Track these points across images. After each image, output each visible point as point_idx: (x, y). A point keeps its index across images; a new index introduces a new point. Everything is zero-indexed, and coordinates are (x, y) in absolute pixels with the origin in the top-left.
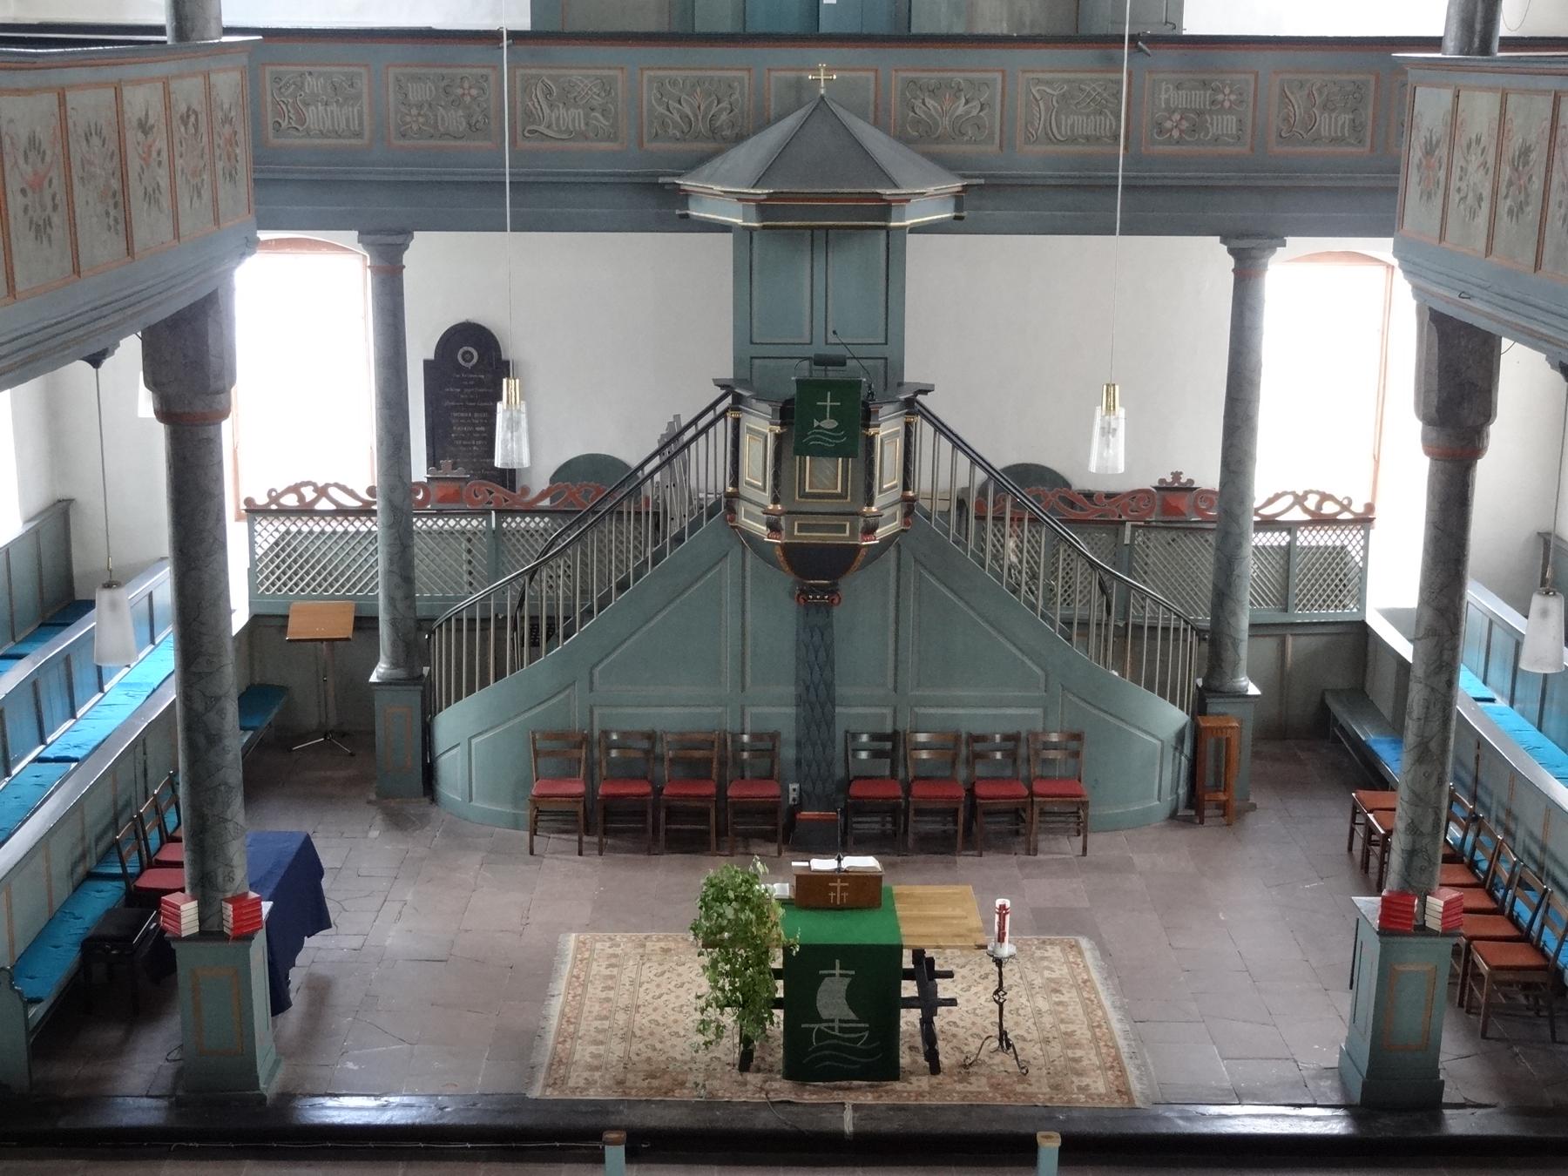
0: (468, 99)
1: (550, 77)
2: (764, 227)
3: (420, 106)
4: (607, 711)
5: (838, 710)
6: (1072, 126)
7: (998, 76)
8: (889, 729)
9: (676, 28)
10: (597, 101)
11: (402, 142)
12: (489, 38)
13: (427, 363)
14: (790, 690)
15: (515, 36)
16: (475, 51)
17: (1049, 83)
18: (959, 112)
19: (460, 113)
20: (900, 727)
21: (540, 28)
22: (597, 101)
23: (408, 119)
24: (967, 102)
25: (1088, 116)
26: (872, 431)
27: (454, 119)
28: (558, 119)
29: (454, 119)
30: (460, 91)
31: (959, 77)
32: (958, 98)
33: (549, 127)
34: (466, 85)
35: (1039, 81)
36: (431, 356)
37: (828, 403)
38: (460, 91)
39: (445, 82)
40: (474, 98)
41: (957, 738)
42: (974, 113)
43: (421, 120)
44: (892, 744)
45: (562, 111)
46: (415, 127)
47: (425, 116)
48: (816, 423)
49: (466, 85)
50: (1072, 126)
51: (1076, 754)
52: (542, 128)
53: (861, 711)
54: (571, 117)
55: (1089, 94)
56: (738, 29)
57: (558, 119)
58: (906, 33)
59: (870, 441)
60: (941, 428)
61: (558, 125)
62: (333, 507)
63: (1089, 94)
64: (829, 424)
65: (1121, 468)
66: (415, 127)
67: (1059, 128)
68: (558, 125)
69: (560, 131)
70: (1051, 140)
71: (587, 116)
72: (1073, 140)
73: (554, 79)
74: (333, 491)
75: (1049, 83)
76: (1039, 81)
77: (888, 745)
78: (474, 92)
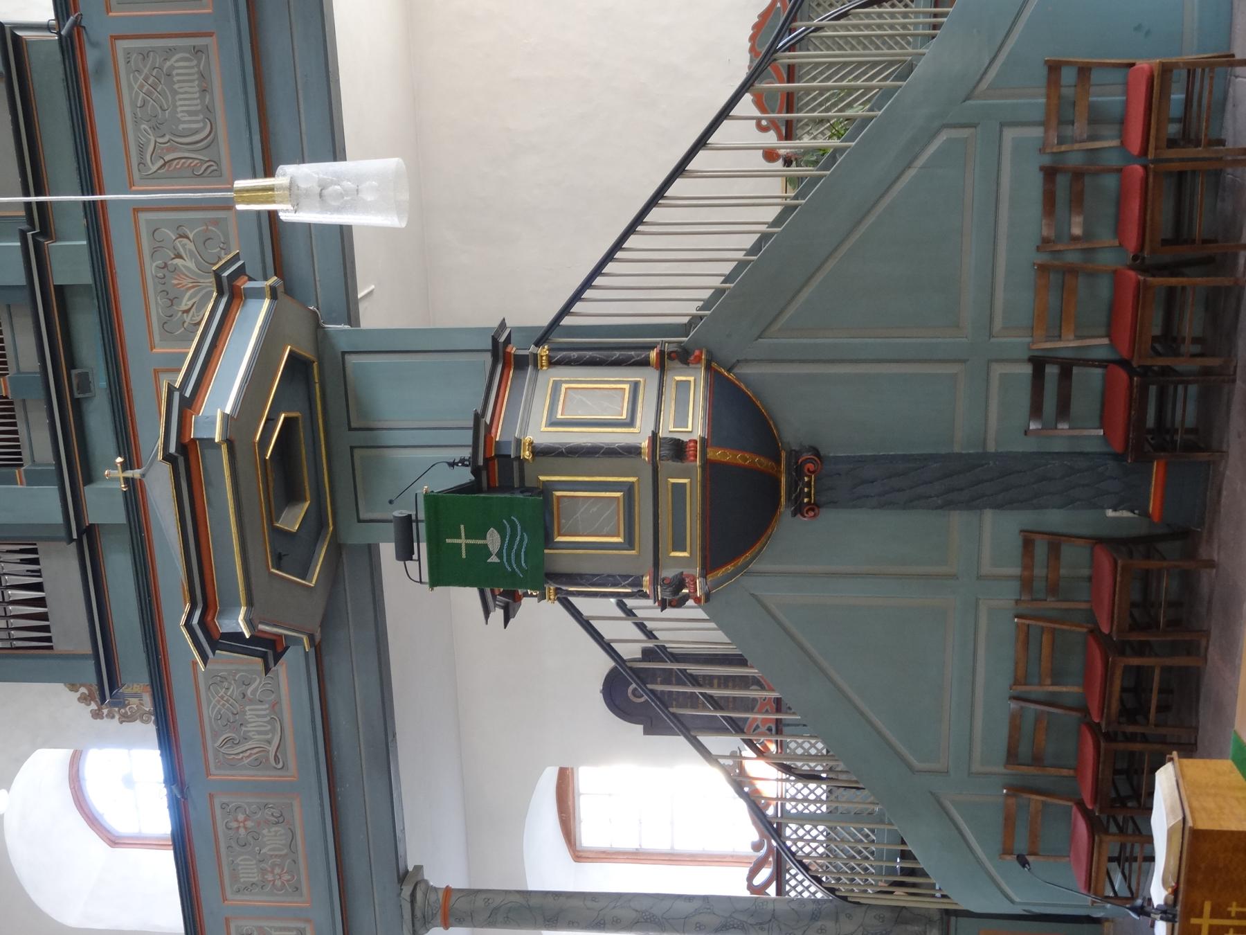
0: (249, 824)
1: (214, 742)
2: (250, 603)
3: (263, 872)
4: (977, 754)
5: (991, 448)
6: (190, 113)
7: (143, 217)
8: (1027, 369)
10: (234, 690)
11: (305, 889)
13: (646, 732)
14: (957, 519)
17: (141, 149)
18: (191, 265)
19: (265, 832)
20: (1026, 356)
22: (234, 690)
23: (278, 883)
24: (179, 256)
25: (175, 93)
26: (527, 454)
27: (273, 839)
28: (259, 733)
29: (273, 839)
30: (242, 831)
31: (151, 268)
32: (176, 268)
33: (269, 742)
34: (235, 825)
35: (142, 163)
36: (640, 728)
37: (463, 541)
38: (242, 831)
39: (234, 844)
40: (247, 818)
41: (1043, 269)
42: (191, 246)
43: (277, 871)
44: (1050, 378)
45: (250, 727)
46: (286, 877)
47: (274, 866)
48: (494, 559)
49: (235, 825)
50: (190, 113)
51: (1084, 71)
52: (272, 749)
53: (995, 416)
54: (256, 717)
55: (149, 94)
57: (259, 733)
59: (541, 452)
60: (566, 310)
61: (266, 733)
62: (774, 884)
63: (149, 94)
64: (493, 540)
65: (392, 164)
66: (286, 877)
67: (196, 132)
68: (266, 733)
69: (273, 730)
70: (211, 142)
71: (251, 702)
72: (209, 110)
73: (216, 735)
74: (759, 880)
75: (141, 149)
76: (142, 163)
77: (1052, 371)
78: (241, 817)
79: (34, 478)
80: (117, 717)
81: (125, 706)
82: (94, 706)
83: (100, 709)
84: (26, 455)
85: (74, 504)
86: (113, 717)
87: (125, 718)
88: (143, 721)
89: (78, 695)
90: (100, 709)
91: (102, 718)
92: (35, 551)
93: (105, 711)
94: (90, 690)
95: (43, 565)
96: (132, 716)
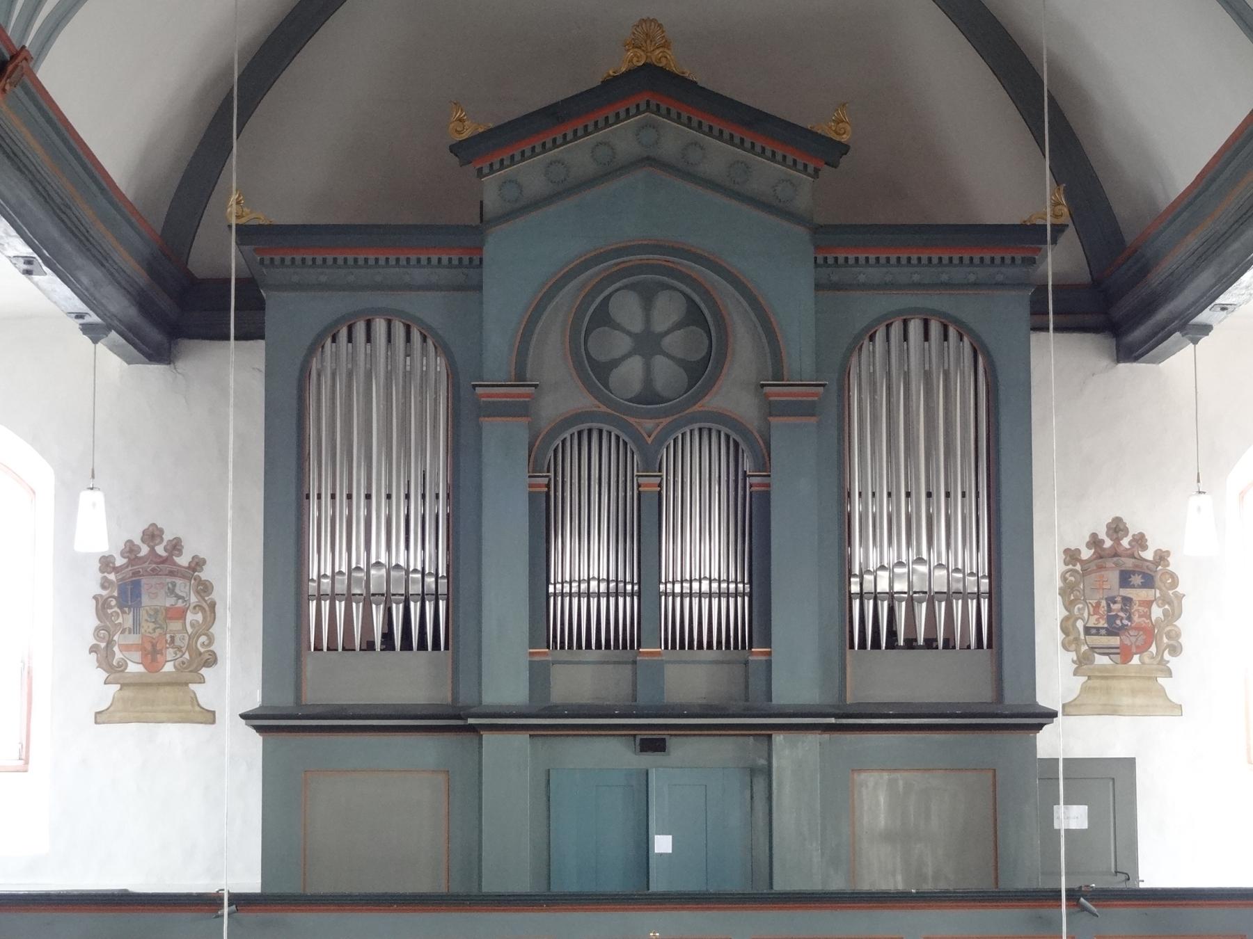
9: (457, 889)
12: (206, 903)
15: (241, 901)
16: (184, 918)
21: (270, 891)
56: (540, 889)
58: (475, 891)
79: (539, 675)
80: (104, 593)
81: (121, 607)
82: (120, 561)
83: (116, 570)
84: (564, 655)
85: (505, 721)
86: (103, 587)
87: (102, 606)
88: (97, 629)
89: (138, 541)
90: (116, 570)
91: (102, 571)
92: (436, 646)
93: (112, 577)
94: (143, 560)
95: (415, 655)
96: (106, 614)
